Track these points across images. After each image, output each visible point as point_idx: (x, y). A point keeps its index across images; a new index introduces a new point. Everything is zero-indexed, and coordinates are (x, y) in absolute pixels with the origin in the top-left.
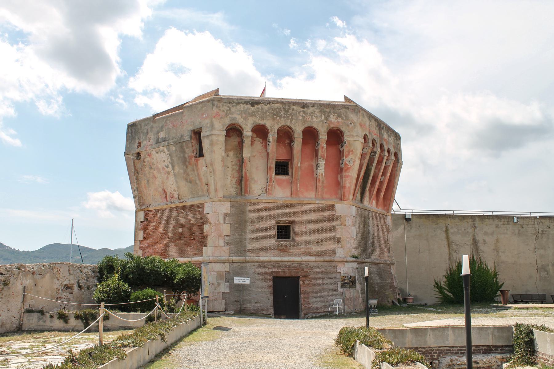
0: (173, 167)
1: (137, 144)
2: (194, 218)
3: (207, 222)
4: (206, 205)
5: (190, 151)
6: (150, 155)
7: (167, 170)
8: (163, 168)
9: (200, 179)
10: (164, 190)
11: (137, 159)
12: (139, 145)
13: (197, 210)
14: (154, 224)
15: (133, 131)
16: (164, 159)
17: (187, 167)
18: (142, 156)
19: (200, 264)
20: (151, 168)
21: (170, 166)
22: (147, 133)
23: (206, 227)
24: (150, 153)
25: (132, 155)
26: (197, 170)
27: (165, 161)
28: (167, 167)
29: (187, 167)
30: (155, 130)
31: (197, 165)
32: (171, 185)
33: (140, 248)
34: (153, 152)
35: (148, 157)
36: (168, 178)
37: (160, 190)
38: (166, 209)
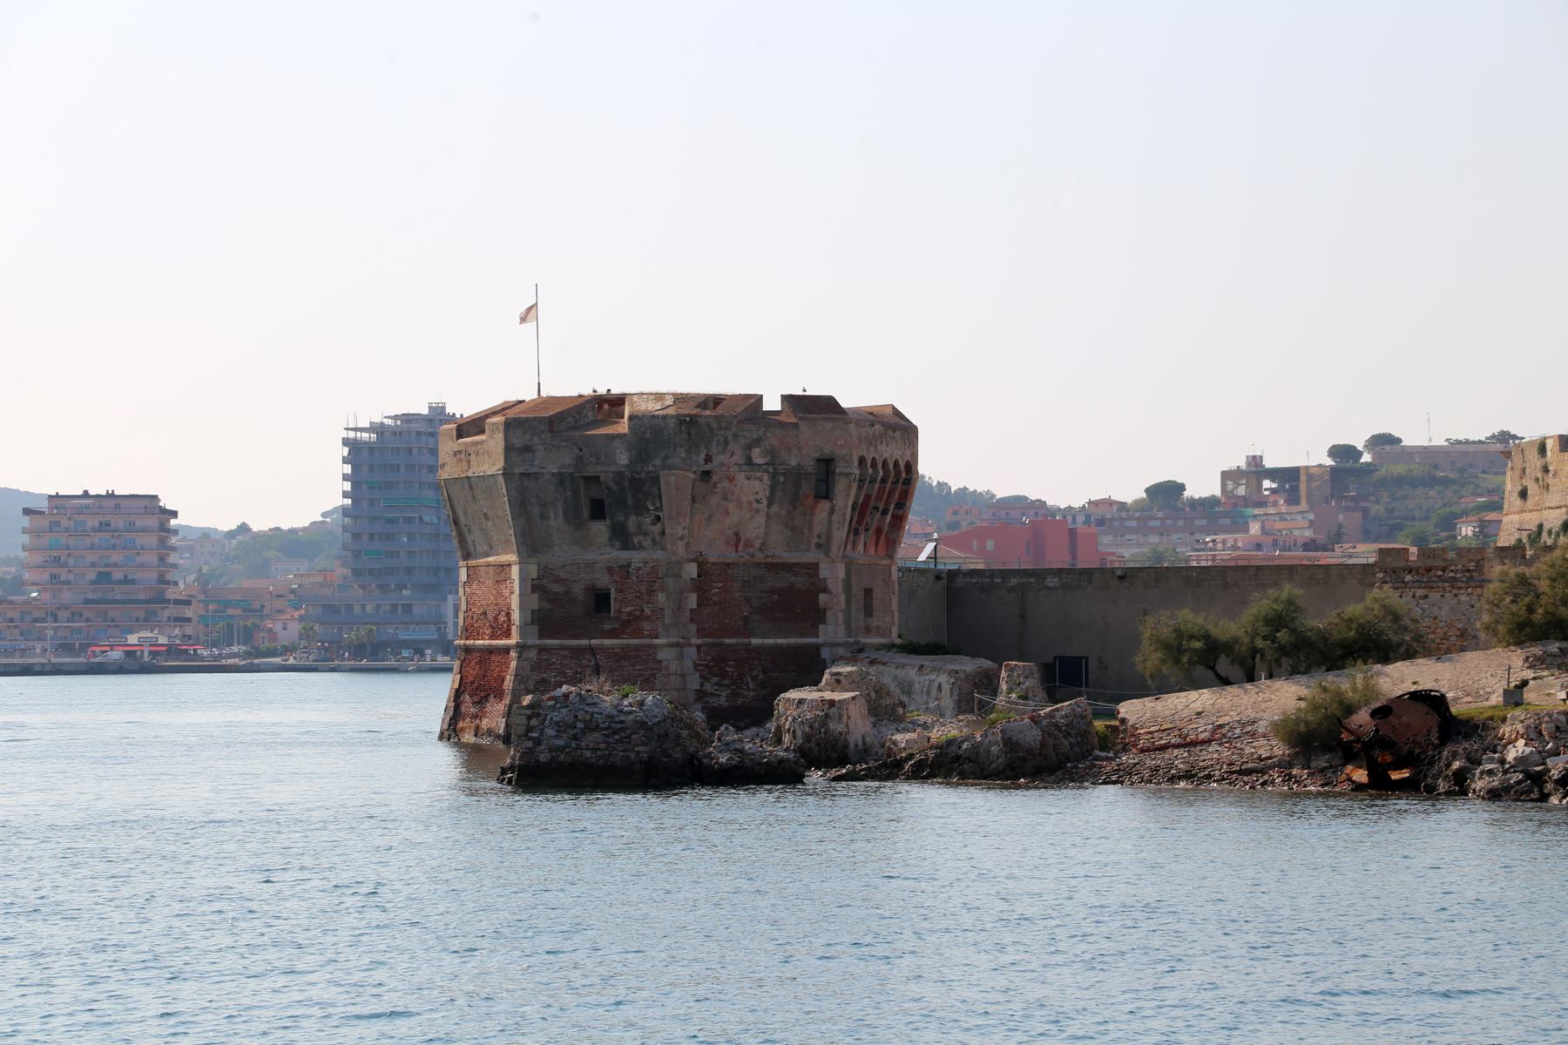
0: (770, 504)
1: (703, 456)
2: (800, 582)
3: (825, 590)
4: (822, 566)
5: (807, 489)
6: (731, 479)
7: (756, 506)
8: (750, 503)
9: (811, 528)
10: (737, 534)
11: (702, 480)
12: (708, 459)
13: (805, 571)
14: (721, 585)
15: (693, 432)
16: (758, 490)
17: (795, 508)
18: (715, 478)
19: (816, 649)
20: (725, 498)
21: (765, 502)
22: (726, 443)
23: (823, 598)
24: (734, 477)
25: (694, 472)
26: (812, 514)
27: (757, 493)
28: (758, 502)
29: (795, 508)
30: (742, 441)
31: (813, 509)
32: (755, 528)
33: (692, 620)
34: (741, 477)
35: (727, 481)
36: (752, 518)
37: (730, 533)
38: (745, 564)
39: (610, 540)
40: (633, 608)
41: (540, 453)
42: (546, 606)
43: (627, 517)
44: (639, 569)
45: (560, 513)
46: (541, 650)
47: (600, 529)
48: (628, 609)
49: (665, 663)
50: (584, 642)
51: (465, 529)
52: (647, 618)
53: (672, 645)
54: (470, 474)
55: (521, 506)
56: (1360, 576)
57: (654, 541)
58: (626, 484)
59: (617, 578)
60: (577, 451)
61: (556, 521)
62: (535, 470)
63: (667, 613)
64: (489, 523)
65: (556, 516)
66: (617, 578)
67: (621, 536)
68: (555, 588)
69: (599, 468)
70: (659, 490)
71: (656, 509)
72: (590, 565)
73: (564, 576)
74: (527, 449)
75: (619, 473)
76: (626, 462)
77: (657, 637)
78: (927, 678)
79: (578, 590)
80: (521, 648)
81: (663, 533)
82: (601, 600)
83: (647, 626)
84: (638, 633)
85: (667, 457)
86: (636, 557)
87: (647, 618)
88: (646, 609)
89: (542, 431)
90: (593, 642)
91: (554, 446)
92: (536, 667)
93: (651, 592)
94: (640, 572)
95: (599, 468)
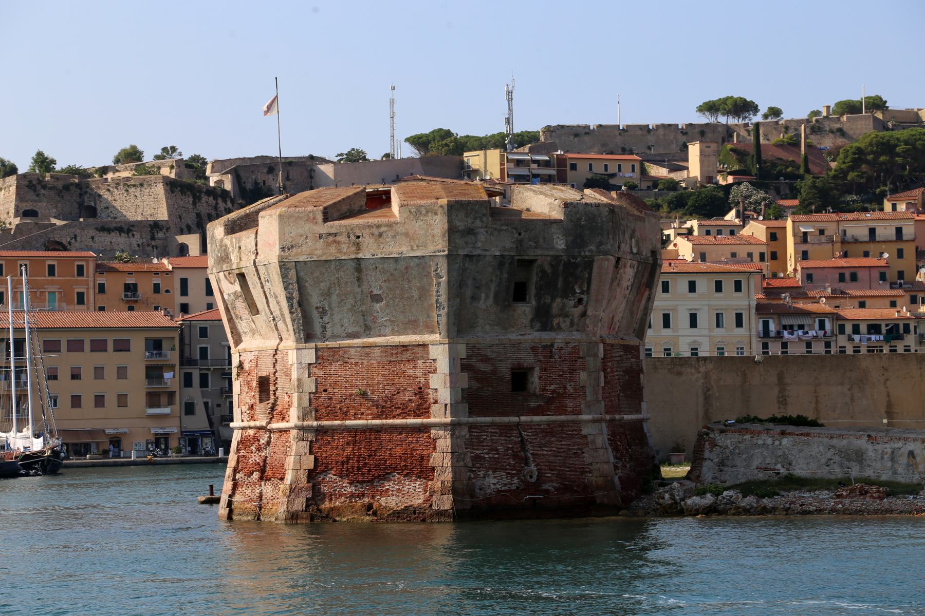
39: (532, 321)
40: (557, 386)
41: (482, 237)
42: (475, 385)
43: (553, 299)
44: (561, 349)
45: (492, 295)
46: (471, 427)
47: (524, 311)
48: (552, 387)
49: (590, 439)
50: (514, 419)
51: (315, 315)
52: (570, 396)
53: (594, 421)
54: (360, 256)
55: (457, 288)
56: (669, 367)
57: (572, 324)
58: (561, 268)
59: (541, 357)
60: (516, 235)
61: (486, 303)
62: (478, 252)
63: (589, 390)
64: (378, 306)
65: (487, 297)
66: (541, 357)
67: (543, 319)
68: (483, 367)
69: (539, 252)
70: (590, 274)
71: (582, 293)
72: (517, 345)
73: (491, 355)
74: (470, 232)
75: (557, 258)
76: (563, 246)
77: (580, 413)
78: (887, 446)
79: (505, 370)
80: (453, 427)
81: (584, 314)
82: (520, 377)
83: (570, 403)
84: (562, 410)
85: (601, 243)
86: (559, 338)
87: (570, 396)
88: (568, 387)
89: (484, 215)
90: (523, 418)
91: (495, 229)
92: (470, 444)
93: (573, 371)
94: (563, 351)
95: (539, 252)
